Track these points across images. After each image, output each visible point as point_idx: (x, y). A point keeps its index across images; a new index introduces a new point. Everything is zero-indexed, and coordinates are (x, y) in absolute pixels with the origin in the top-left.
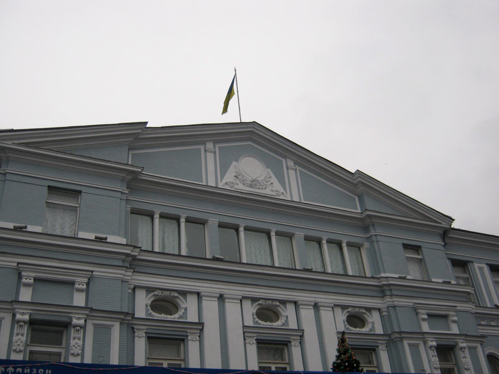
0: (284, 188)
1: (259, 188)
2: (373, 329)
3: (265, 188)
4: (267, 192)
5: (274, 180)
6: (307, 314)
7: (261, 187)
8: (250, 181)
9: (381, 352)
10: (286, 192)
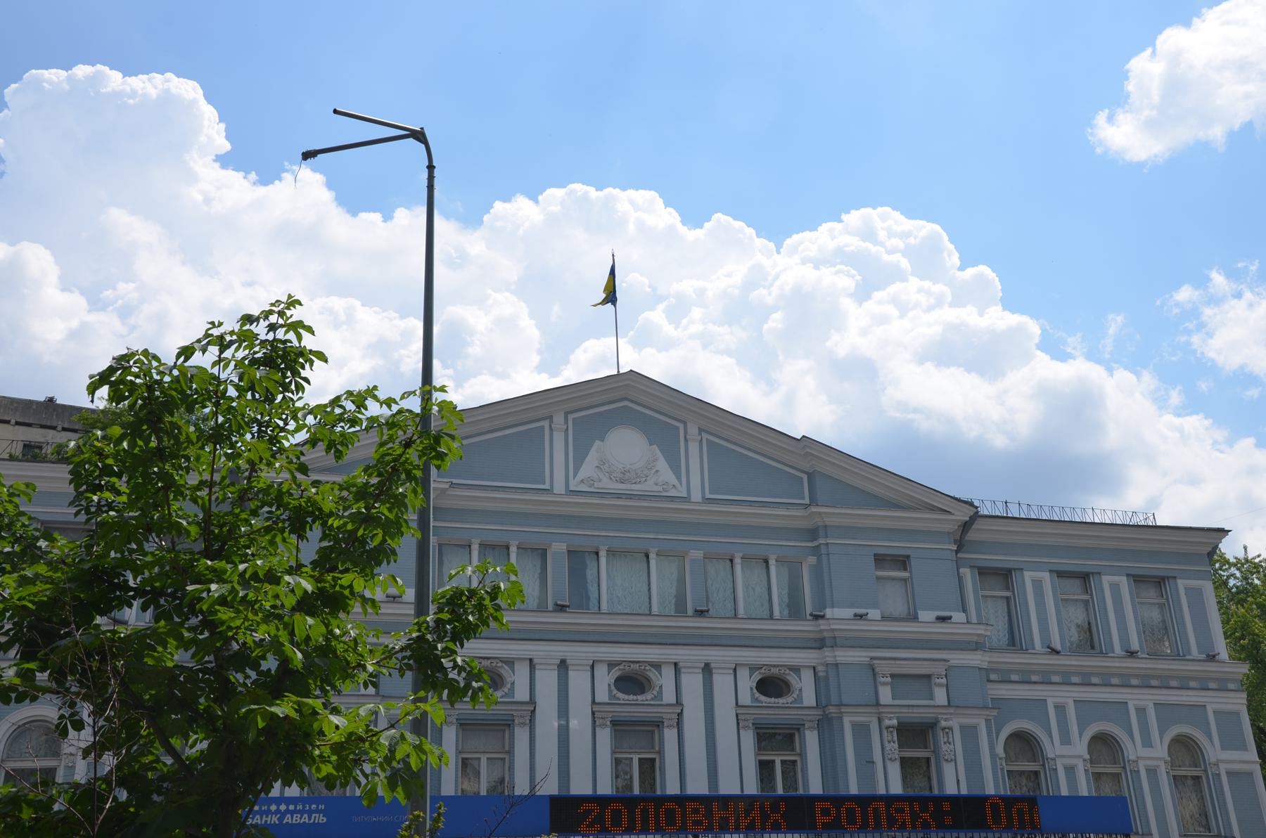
0: (679, 478)
1: (635, 483)
2: (799, 699)
3: (646, 480)
4: (649, 487)
5: (662, 464)
6: (693, 683)
7: (638, 480)
8: (621, 472)
9: (666, 731)
10: (681, 484)
